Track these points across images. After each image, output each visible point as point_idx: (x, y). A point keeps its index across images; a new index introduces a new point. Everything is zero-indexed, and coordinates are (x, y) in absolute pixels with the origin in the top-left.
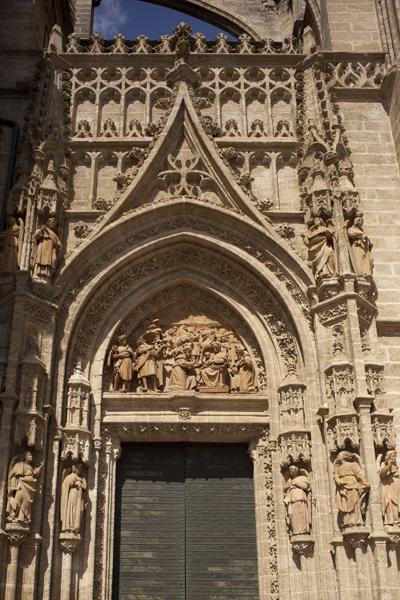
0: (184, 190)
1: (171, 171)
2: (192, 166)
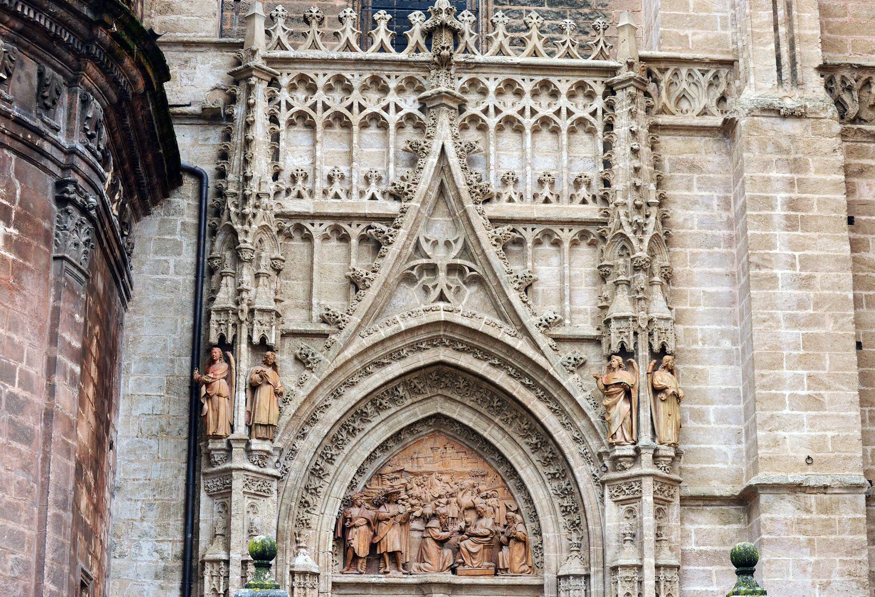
0: (442, 292)
1: (425, 261)
2: (454, 253)
